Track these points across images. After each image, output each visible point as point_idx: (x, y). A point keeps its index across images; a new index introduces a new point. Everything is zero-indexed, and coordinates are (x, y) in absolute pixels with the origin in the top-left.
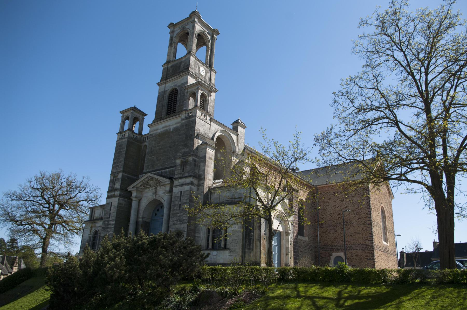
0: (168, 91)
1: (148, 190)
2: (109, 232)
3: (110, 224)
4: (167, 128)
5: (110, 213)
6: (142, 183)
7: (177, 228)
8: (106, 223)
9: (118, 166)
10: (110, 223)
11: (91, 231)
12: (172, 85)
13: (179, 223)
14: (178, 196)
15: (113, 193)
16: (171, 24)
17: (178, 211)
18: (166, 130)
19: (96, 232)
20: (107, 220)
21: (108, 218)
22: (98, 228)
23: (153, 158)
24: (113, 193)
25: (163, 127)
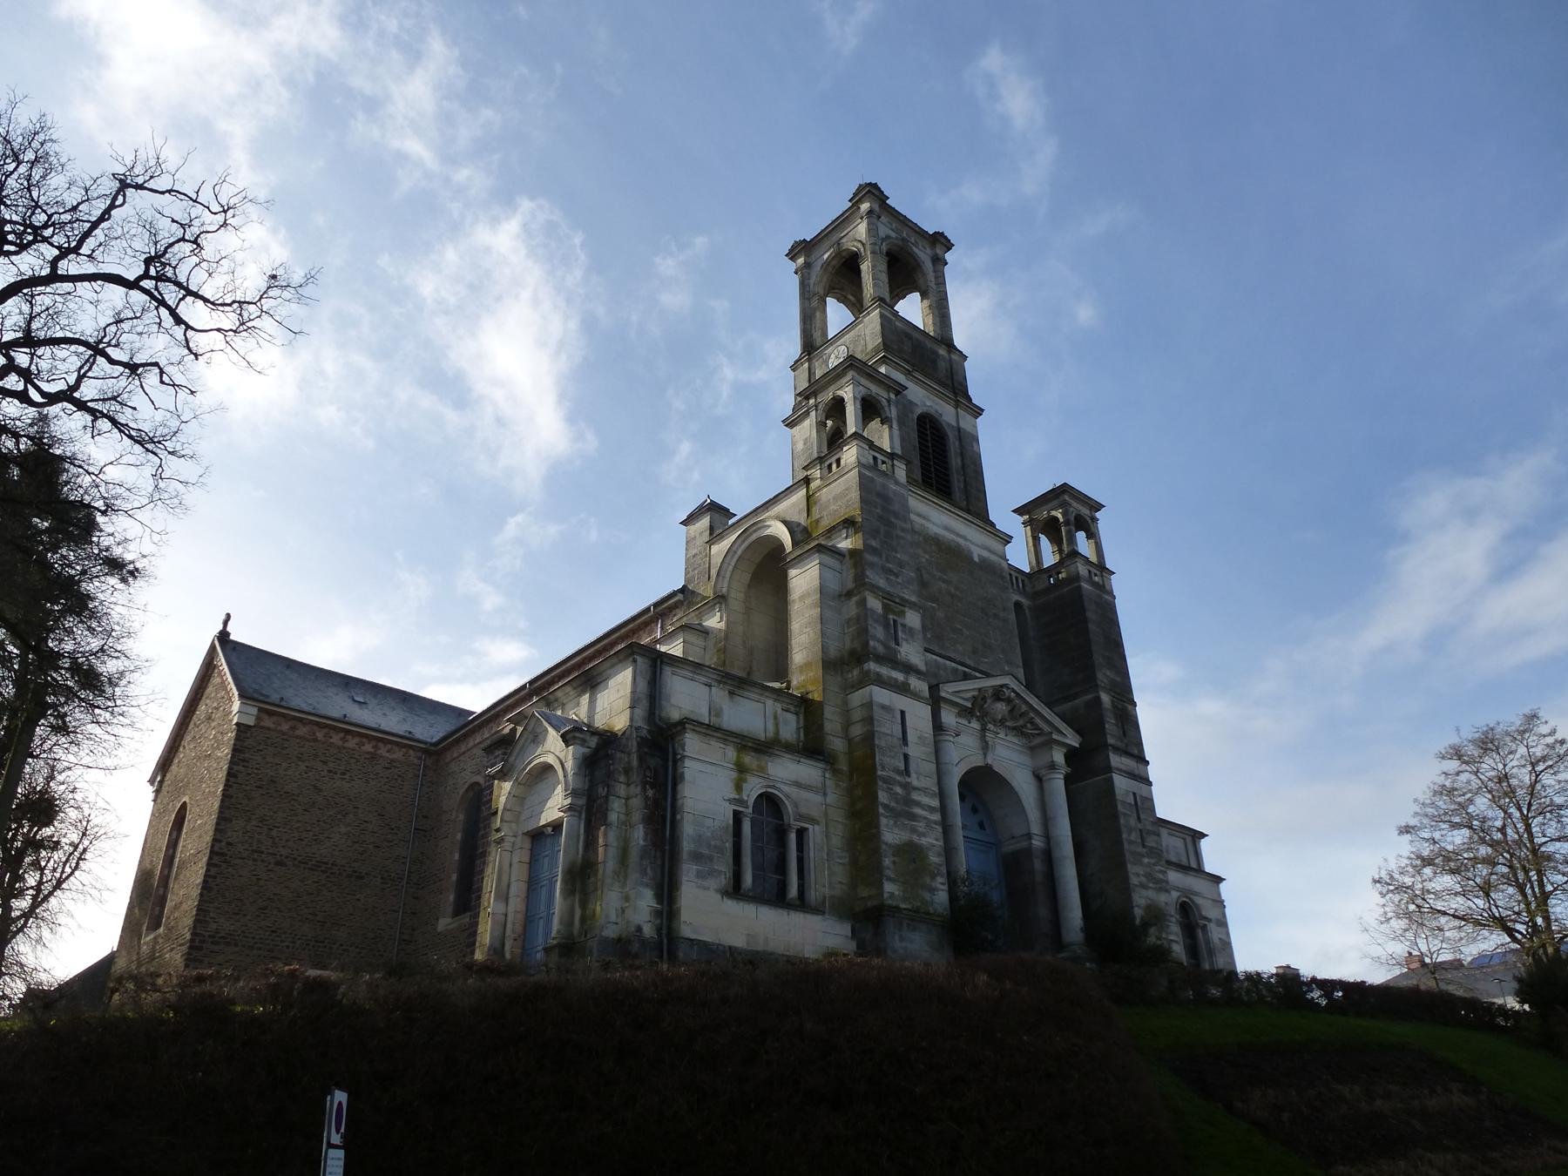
0: (919, 411)
1: (966, 723)
2: (924, 835)
3: (918, 804)
4: (961, 541)
5: (906, 757)
6: (976, 693)
7: (1152, 900)
8: (899, 790)
9: (890, 571)
10: (915, 796)
11: (738, 787)
12: (928, 403)
13: (1151, 885)
14: (1130, 804)
15: (900, 676)
16: (875, 186)
17: (1141, 850)
18: (958, 545)
19: (770, 803)
20: (898, 778)
21: (898, 771)
22: (786, 789)
23: (933, 608)
24: (900, 676)
25: (946, 528)
